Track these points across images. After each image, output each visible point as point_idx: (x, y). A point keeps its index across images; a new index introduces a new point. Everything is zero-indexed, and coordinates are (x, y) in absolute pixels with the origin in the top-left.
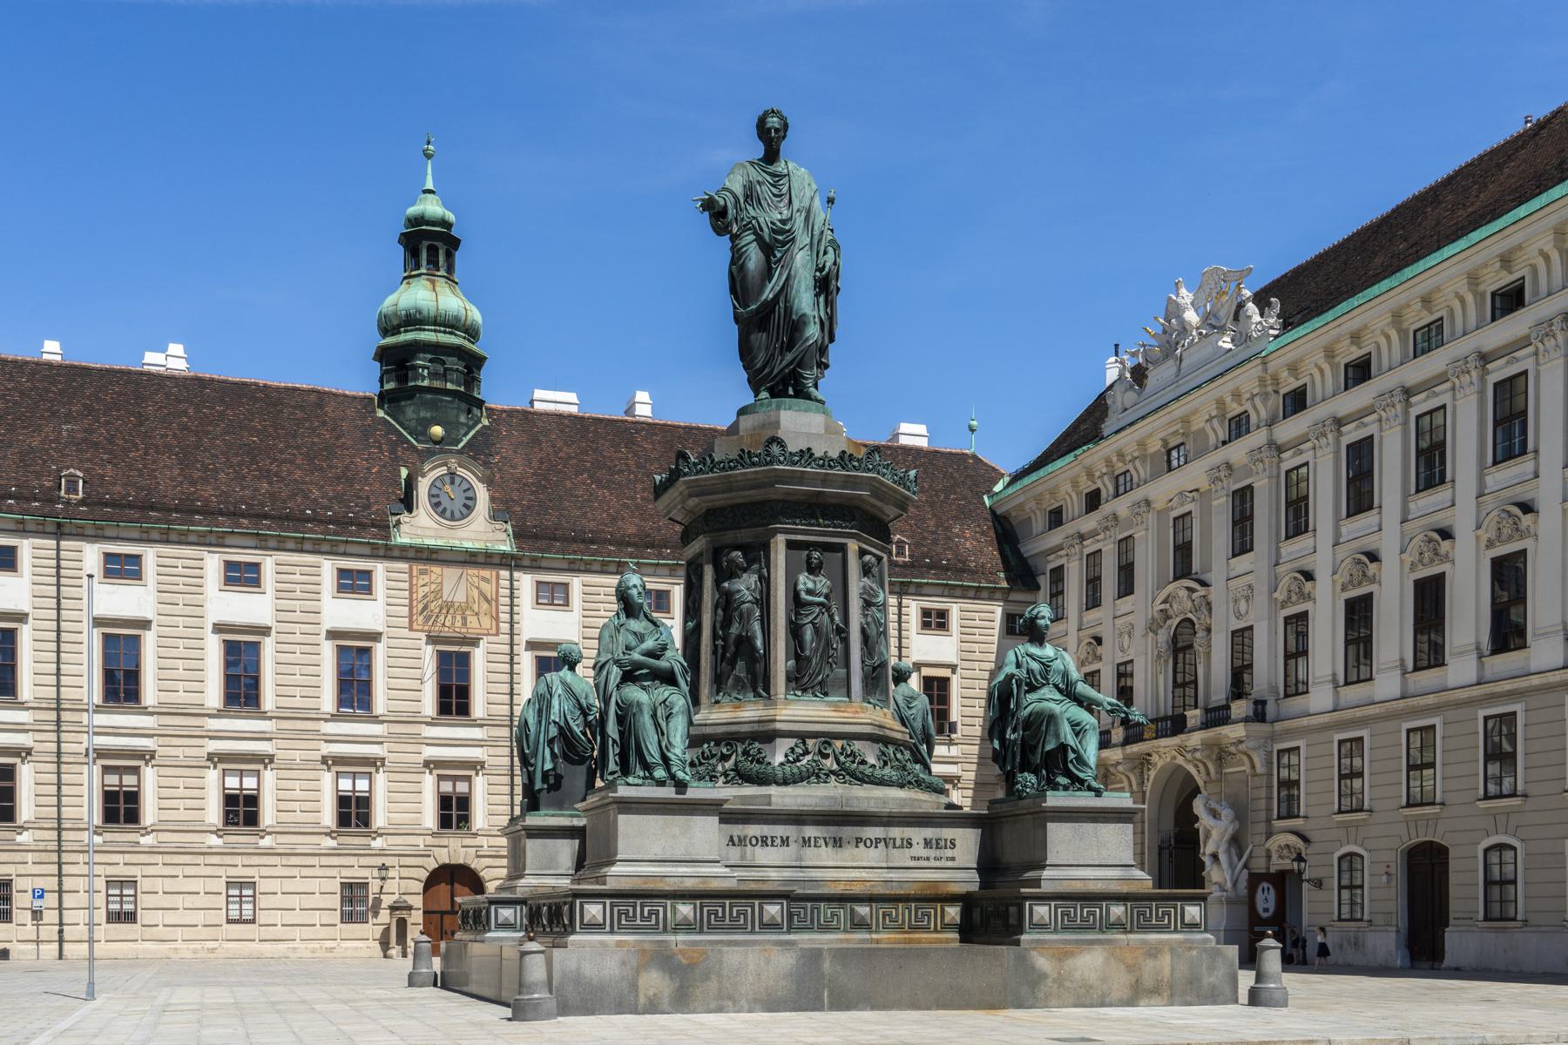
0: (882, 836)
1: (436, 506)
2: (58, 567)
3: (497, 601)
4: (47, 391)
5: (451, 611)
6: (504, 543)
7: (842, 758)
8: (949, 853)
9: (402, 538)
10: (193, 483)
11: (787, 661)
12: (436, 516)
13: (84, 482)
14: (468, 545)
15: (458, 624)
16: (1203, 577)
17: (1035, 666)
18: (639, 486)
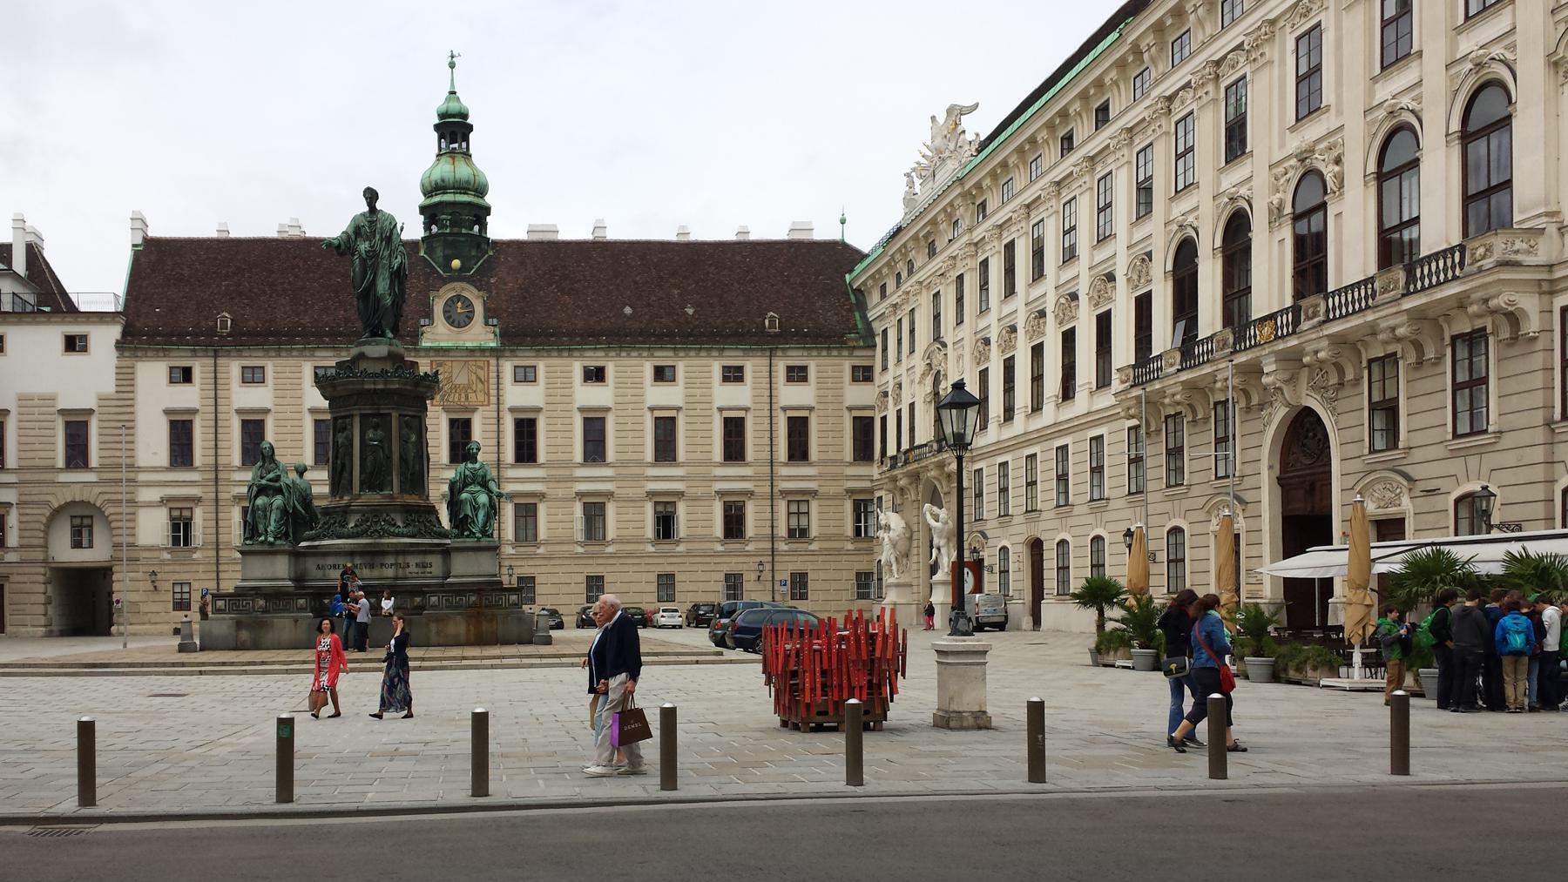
0: (393, 562)
1: (448, 318)
2: (216, 378)
3: (488, 382)
4: (216, 258)
5: (458, 391)
6: (493, 344)
7: (383, 523)
8: (428, 570)
9: (425, 344)
10: (298, 315)
11: (361, 474)
12: (449, 326)
13: (232, 320)
14: (469, 344)
15: (463, 399)
16: (945, 340)
17: (467, 473)
18: (590, 291)
